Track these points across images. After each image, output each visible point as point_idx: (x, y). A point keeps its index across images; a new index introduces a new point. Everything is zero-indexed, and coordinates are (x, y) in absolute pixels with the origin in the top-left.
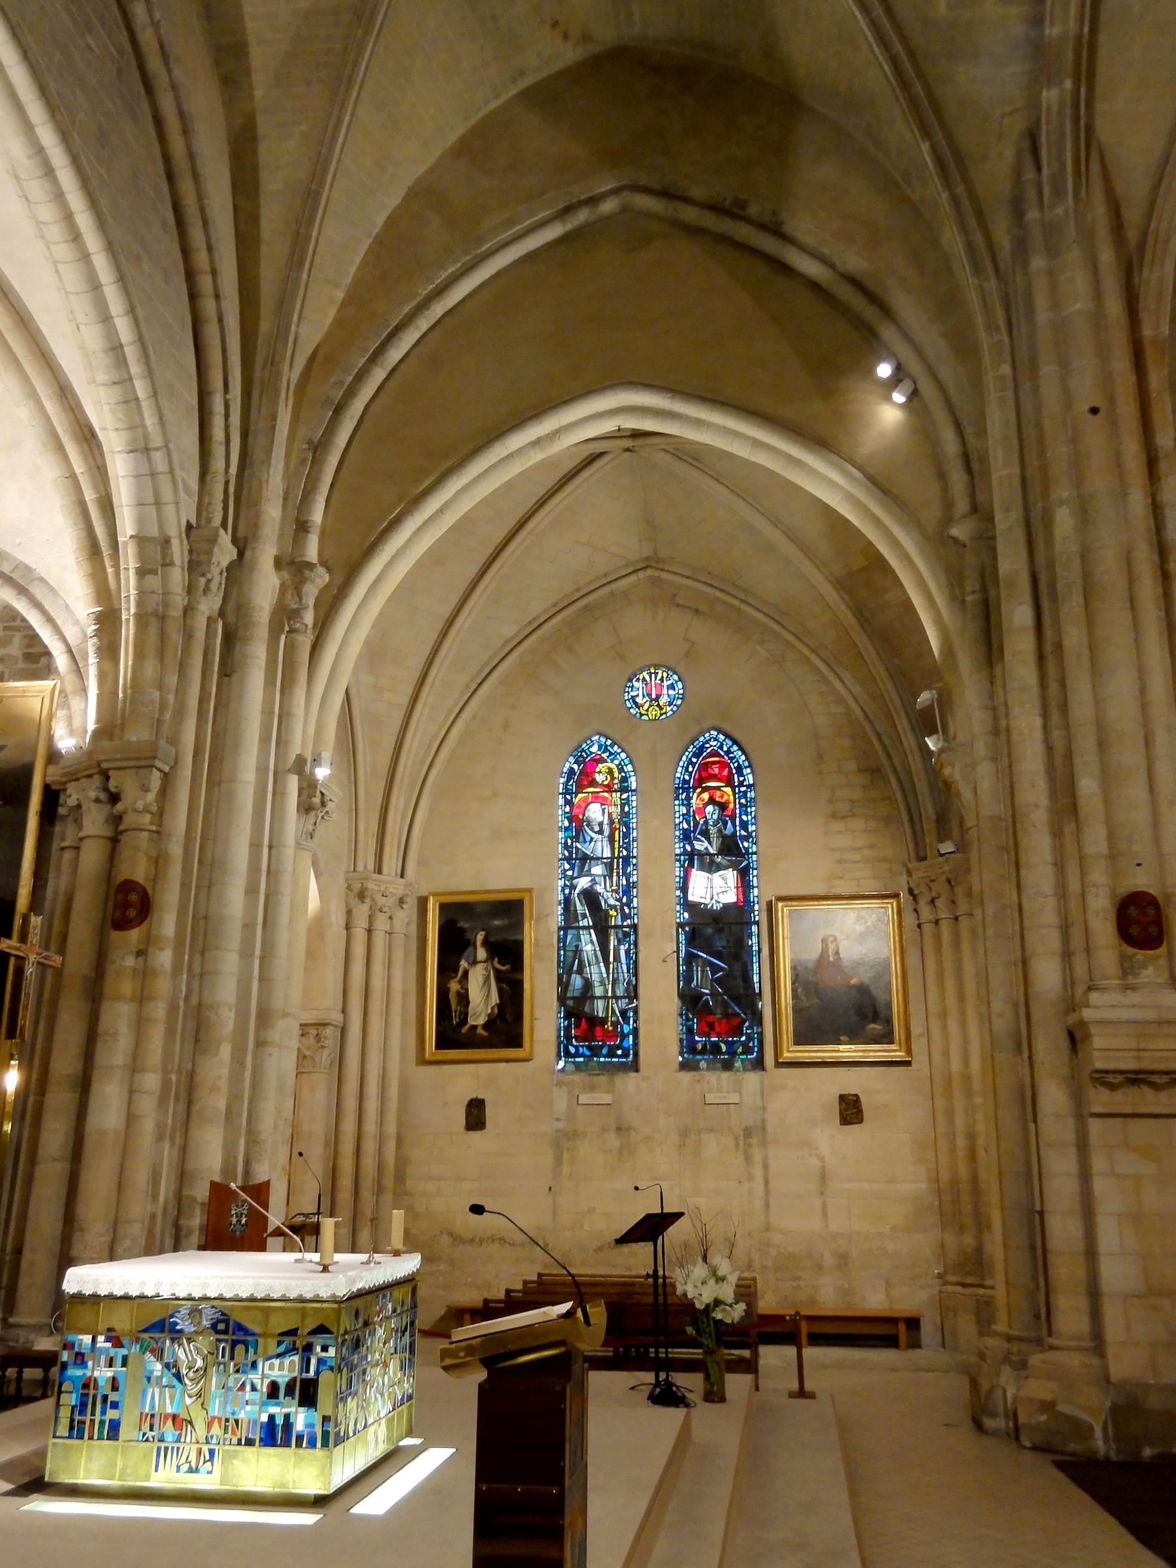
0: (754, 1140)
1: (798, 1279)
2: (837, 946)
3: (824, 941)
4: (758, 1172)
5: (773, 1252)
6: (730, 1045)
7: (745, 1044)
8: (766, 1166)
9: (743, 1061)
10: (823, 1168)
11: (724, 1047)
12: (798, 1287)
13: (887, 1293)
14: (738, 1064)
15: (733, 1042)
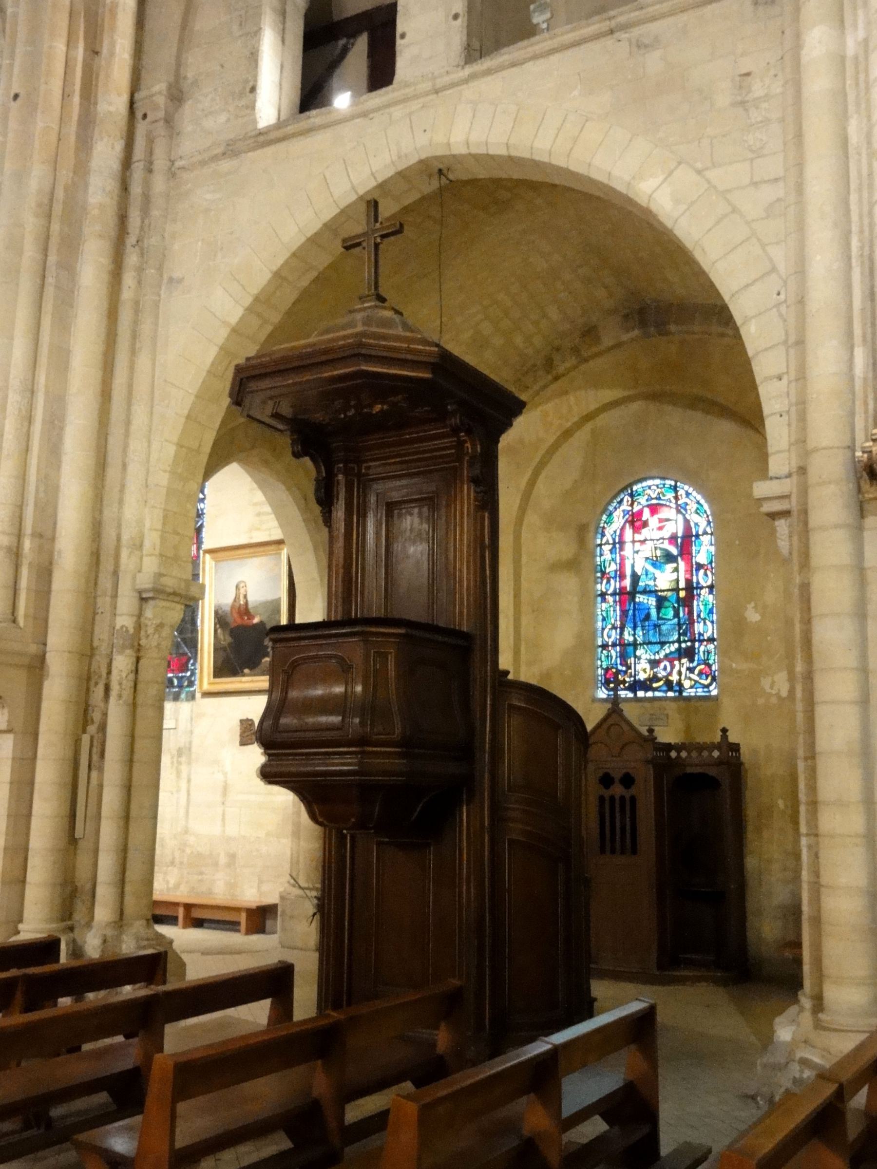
0: (183, 759)
1: (201, 873)
2: (246, 591)
3: (237, 587)
4: (184, 784)
5: (188, 851)
6: (180, 679)
7: (189, 678)
8: (189, 781)
9: (187, 692)
10: (225, 782)
11: (176, 682)
12: (201, 881)
13: (259, 887)
14: (183, 696)
15: (182, 677)
